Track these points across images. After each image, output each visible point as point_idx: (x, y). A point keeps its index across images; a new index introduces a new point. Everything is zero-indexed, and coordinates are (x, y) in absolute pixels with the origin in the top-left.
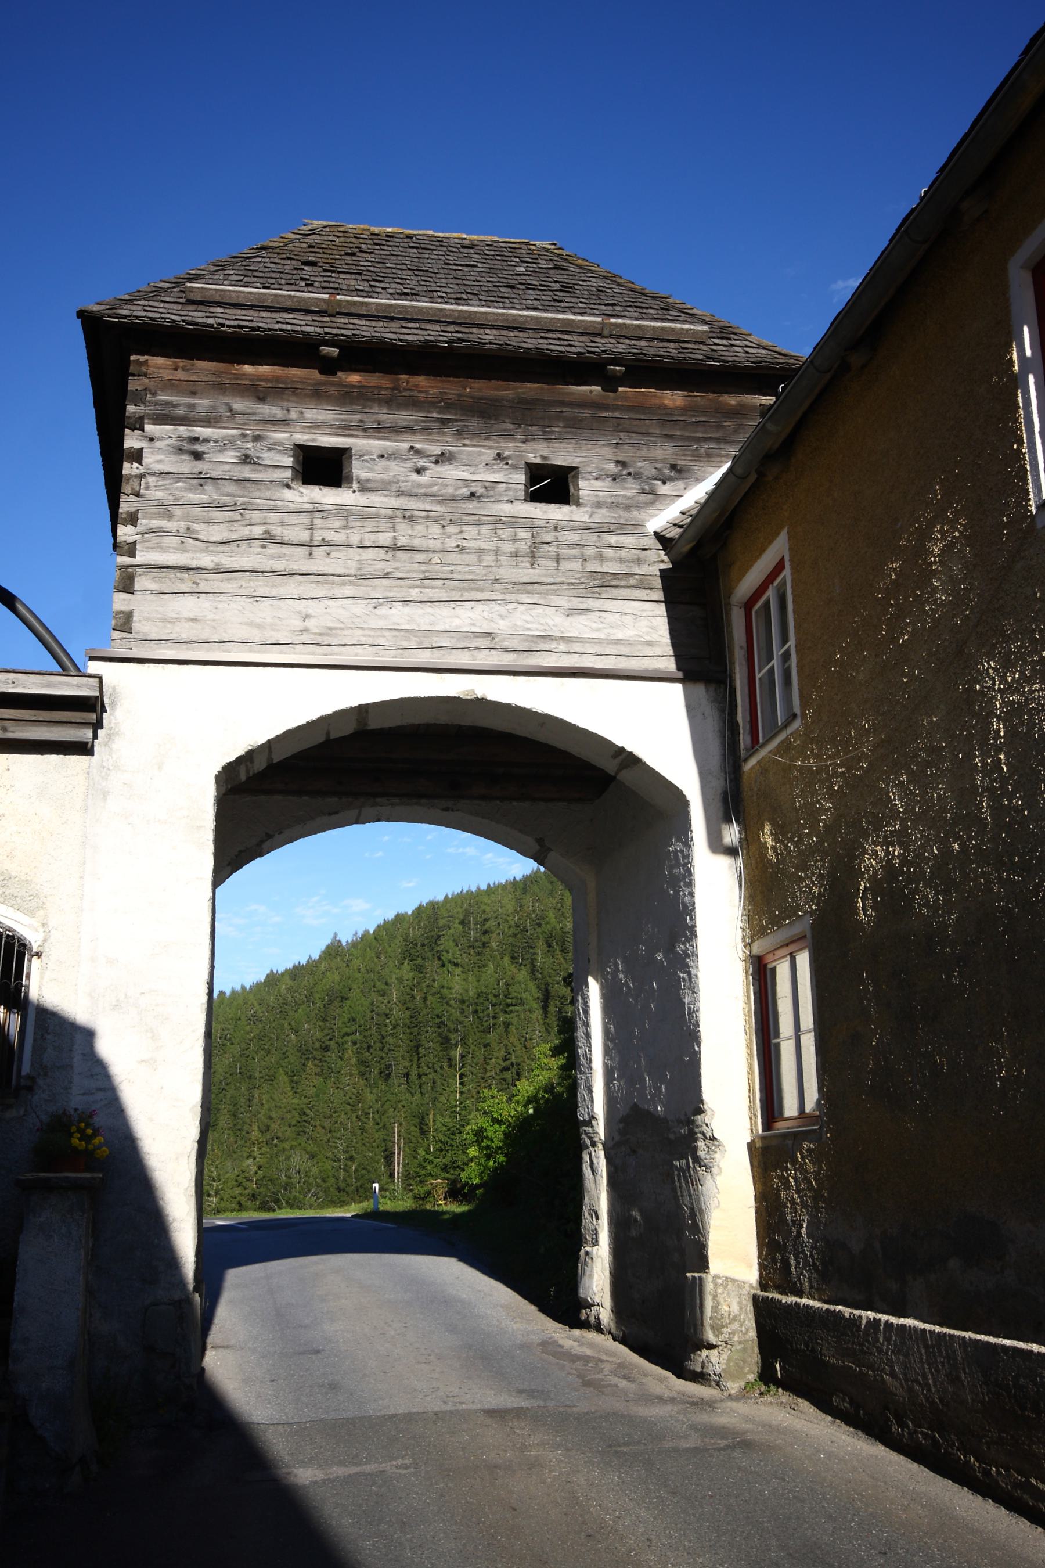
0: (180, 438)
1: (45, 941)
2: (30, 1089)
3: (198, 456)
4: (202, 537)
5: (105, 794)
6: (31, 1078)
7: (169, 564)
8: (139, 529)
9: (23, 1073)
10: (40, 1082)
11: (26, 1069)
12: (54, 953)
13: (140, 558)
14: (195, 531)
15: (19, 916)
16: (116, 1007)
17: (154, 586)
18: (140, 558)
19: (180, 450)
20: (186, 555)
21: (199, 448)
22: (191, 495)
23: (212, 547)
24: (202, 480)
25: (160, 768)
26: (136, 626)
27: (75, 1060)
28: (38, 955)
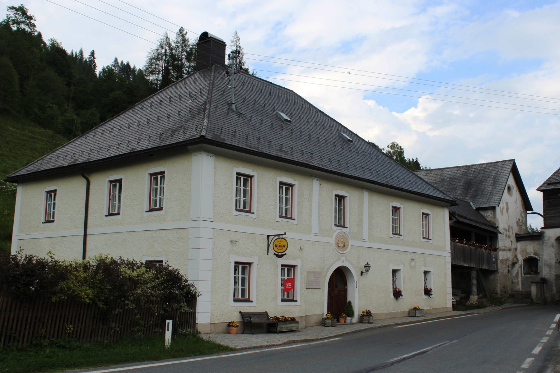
5: (544, 243)
11: (539, 271)
12: (541, 260)
15: (537, 257)
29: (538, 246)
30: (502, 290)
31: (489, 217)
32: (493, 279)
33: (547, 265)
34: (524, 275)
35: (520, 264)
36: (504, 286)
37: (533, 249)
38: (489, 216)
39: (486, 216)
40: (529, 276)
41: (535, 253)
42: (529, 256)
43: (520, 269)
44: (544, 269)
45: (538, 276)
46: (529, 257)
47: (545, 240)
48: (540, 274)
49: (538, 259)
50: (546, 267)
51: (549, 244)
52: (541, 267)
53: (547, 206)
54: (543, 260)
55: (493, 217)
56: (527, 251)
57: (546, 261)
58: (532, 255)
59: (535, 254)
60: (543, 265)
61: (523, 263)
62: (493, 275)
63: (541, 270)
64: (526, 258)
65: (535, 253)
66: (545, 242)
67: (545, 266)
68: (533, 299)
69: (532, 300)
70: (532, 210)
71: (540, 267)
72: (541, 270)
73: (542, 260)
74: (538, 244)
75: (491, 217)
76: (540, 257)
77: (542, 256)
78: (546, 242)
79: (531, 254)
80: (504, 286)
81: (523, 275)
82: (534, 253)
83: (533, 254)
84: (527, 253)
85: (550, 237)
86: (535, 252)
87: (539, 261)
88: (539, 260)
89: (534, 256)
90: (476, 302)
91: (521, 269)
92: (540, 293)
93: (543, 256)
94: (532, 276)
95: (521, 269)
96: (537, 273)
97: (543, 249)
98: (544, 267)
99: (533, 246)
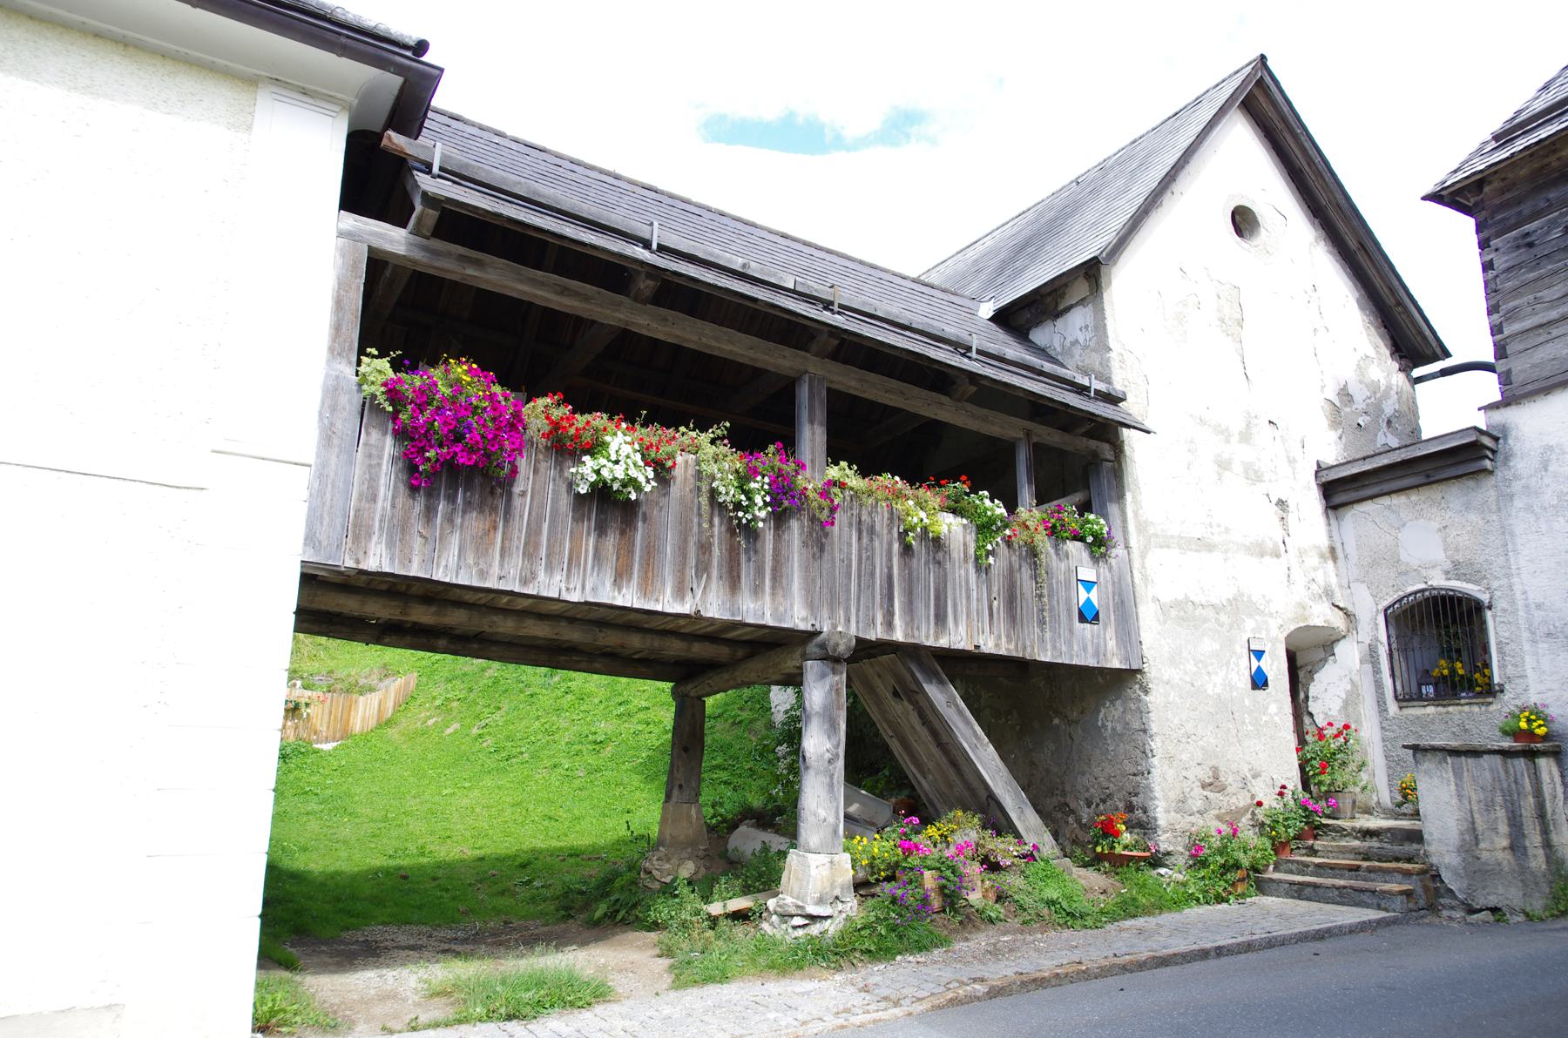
0: (1516, 239)
1: (1491, 598)
2: (1502, 691)
3: (1531, 245)
4: (1547, 300)
5: (1511, 497)
6: (1501, 685)
7: (1528, 327)
8: (1501, 314)
9: (1496, 682)
10: (1507, 686)
11: (1496, 680)
12: (1500, 604)
13: (1507, 332)
14: (1541, 298)
16: (1549, 635)
17: (1521, 347)
18: (1507, 332)
19: (1518, 247)
20: (1537, 317)
21: (1529, 239)
22: (1532, 275)
23: (1556, 303)
24: (1538, 262)
25: (1546, 470)
26: (1513, 378)
27: (1528, 671)
28: (1490, 608)
29: (1473, 517)
30: (1198, 804)
31: (1077, 351)
32: (1119, 728)
33: (1549, 635)
34: (1401, 708)
35: (1368, 641)
36: (1215, 771)
37: (1445, 541)
38: (1077, 341)
39: (1059, 349)
40: (1431, 710)
41: (1456, 565)
42: (1423, 586)
43: (1369, 667)
44: (1528, 658)
45: (1492, 708)
46: (1423, 591)
47: (1517, 477)
48: (1507, 697)
49: (1485, 598)
50: (1543, 646)
51: (1549, 497)
52: (1507, 649)
53: (1508, 270)
54: (1520, 603)
55: (1092, 344)
56: (1404, 557)
57: (1539, 606)
58: (1439, 581)
59: (1456, 570)
60: (1526, 635)
61: (1383, 637)
62: (1118, 703)
63: (1510, 670)
64: (1400, 600)
65: (1456, 565)
66: (1517, 486)
67: (1534, 642)
68: (1446, 876)
69: (1432, 875)
70: (1447, 354)
71: (1501, 651)
72: (1510, 670)
73: (1513, 602)
74: (1468, 506)
75: (1085, 347)
76: (1495, 584)
77: (1508, 576)
78: (1526, 487)
79: (1432, 573)
80: (1215, 771)
81: (1393, 707)
82: (1448, 565)
83: (1447, 573)
84: (1406, 573)
85: (1550, 448)
86: (1460, 557)
87: (1489, 614)
88: (1490, 608)
89: (1455, 584)
90: (813, 910)
91: (1377, 671)
92: (1503, 828)
93: (1515, 580)
94: (1451, 709)
95: (1377, 671)
96: (1489, 691)
97: (1504, 530)
98: (1527, 647)
99: (1435, 525)
